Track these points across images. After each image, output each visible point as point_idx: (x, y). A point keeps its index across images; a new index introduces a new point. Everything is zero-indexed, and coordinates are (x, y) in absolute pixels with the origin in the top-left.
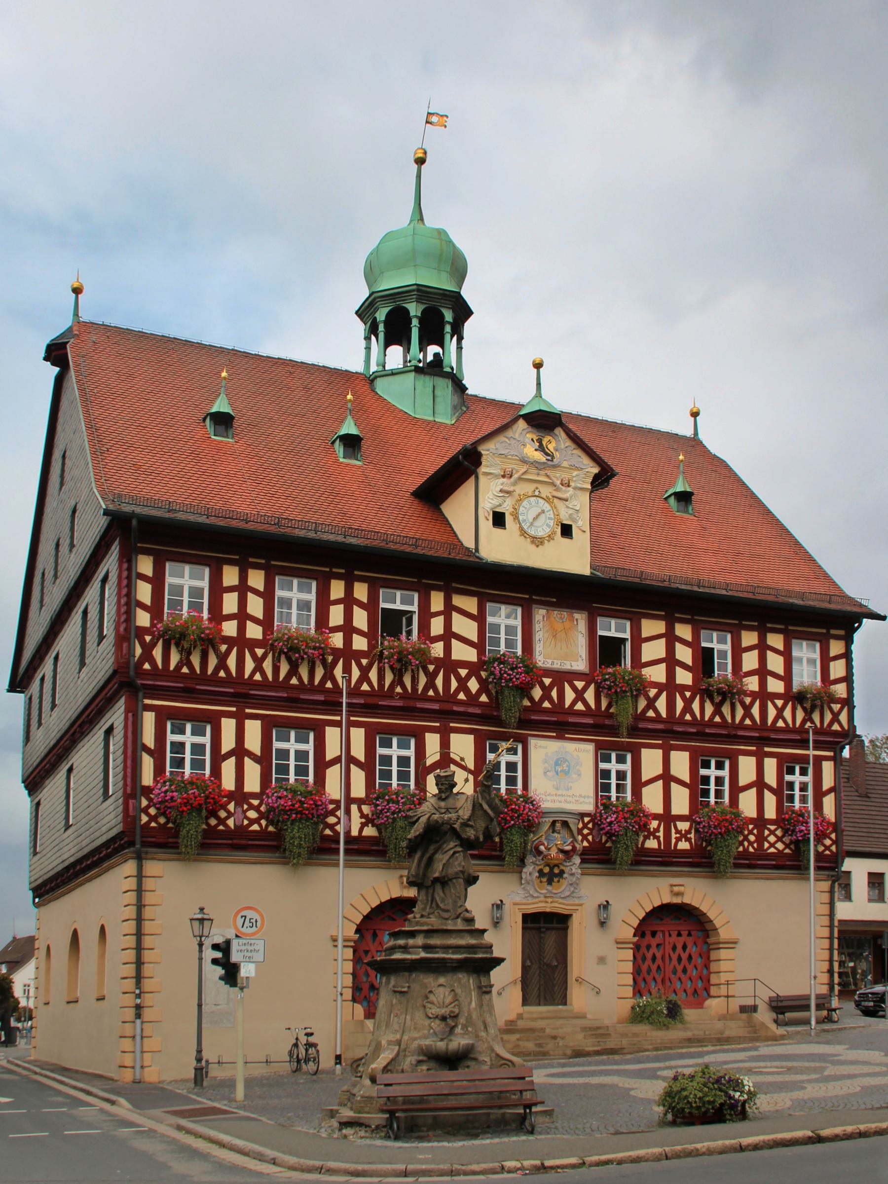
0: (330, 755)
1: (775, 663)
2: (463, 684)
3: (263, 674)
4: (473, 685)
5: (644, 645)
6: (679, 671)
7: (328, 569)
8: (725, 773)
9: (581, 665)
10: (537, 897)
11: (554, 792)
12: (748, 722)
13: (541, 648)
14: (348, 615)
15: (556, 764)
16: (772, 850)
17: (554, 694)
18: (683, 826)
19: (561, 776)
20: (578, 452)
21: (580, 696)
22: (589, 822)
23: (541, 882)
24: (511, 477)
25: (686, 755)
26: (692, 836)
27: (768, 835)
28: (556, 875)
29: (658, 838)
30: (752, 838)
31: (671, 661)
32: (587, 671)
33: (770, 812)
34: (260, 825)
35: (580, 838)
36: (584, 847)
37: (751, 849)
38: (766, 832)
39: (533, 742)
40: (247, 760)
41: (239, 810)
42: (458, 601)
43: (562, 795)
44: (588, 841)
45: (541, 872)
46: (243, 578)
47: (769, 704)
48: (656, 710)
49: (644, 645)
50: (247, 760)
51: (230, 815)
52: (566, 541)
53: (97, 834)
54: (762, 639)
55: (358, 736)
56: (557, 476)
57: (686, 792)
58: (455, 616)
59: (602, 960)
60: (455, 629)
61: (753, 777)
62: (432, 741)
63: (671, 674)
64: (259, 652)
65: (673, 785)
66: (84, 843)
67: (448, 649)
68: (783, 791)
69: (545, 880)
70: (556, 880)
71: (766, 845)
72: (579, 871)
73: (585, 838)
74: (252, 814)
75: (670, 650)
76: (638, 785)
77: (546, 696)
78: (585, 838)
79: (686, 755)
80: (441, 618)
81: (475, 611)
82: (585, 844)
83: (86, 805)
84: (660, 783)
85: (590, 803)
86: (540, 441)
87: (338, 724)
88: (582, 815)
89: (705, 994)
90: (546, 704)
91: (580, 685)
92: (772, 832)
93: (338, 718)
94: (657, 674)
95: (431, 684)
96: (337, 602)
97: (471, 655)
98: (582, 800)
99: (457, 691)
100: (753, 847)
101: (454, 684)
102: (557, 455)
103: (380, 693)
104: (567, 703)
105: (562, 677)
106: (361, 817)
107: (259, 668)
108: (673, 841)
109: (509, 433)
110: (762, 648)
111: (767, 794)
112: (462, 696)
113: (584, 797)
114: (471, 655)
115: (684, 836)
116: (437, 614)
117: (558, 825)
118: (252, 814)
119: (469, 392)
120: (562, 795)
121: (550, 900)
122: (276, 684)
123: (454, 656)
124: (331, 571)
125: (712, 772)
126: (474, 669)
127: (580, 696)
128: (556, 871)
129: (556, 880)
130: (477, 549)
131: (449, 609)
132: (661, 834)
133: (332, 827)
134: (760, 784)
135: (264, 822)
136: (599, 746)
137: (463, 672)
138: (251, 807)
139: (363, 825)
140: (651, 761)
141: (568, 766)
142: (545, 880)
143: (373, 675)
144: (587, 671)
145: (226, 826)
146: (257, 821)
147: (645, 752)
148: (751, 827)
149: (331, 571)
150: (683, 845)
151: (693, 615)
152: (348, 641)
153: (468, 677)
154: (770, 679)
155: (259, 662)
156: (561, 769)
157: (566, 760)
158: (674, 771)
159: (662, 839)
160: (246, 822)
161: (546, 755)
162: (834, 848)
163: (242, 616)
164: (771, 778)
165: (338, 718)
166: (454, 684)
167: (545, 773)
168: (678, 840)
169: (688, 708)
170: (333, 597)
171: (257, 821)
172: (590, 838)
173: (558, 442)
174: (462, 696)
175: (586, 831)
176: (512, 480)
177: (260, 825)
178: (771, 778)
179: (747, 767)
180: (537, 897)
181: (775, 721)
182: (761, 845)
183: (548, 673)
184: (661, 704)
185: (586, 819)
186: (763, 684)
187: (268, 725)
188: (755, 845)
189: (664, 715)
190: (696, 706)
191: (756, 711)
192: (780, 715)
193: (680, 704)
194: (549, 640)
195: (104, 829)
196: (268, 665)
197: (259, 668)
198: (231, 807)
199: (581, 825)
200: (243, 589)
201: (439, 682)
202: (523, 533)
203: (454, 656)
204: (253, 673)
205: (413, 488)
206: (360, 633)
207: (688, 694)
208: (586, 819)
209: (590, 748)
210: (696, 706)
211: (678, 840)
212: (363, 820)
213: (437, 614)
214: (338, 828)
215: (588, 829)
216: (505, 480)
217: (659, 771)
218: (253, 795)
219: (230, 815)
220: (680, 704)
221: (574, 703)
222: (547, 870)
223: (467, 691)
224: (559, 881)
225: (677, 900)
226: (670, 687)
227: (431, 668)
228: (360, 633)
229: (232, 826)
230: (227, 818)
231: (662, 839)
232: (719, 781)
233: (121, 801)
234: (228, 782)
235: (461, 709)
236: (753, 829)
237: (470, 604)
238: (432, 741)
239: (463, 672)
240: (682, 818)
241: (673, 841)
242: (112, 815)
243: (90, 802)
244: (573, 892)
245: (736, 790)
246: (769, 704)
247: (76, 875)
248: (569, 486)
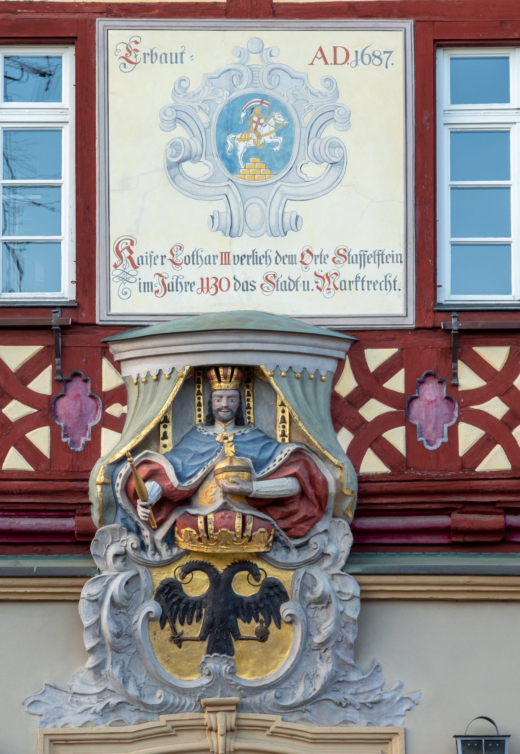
10: (163, 708)
11: (216, 243)
22: (388, 370)
35: (345, 438)
39: (115, 38)
43: (255, 259)
44: (386, 452)
45: (169, 593)
69: (194, 629)
72: (351, 587)
73: (368, 437)
78: (368, 437)
82: (372, 464)
85: (389, 284)
88: (359, 338)
98: (349, 271)
113: (363, 259)
120: (255, 259)
121: (220, 720)
128: (245, 588)
129: (247, 628)
142: (194, 629)
157: (275, 105)
161: (181, 86)
167: (174, 167)
172: (397, 437)
175: (373, 410)
180: (163, 708)
185: (376, 357)
208: (376, 357)
215: (387, 397)
222: (198, 586)
224: (262, 636)
244: (334, 682)
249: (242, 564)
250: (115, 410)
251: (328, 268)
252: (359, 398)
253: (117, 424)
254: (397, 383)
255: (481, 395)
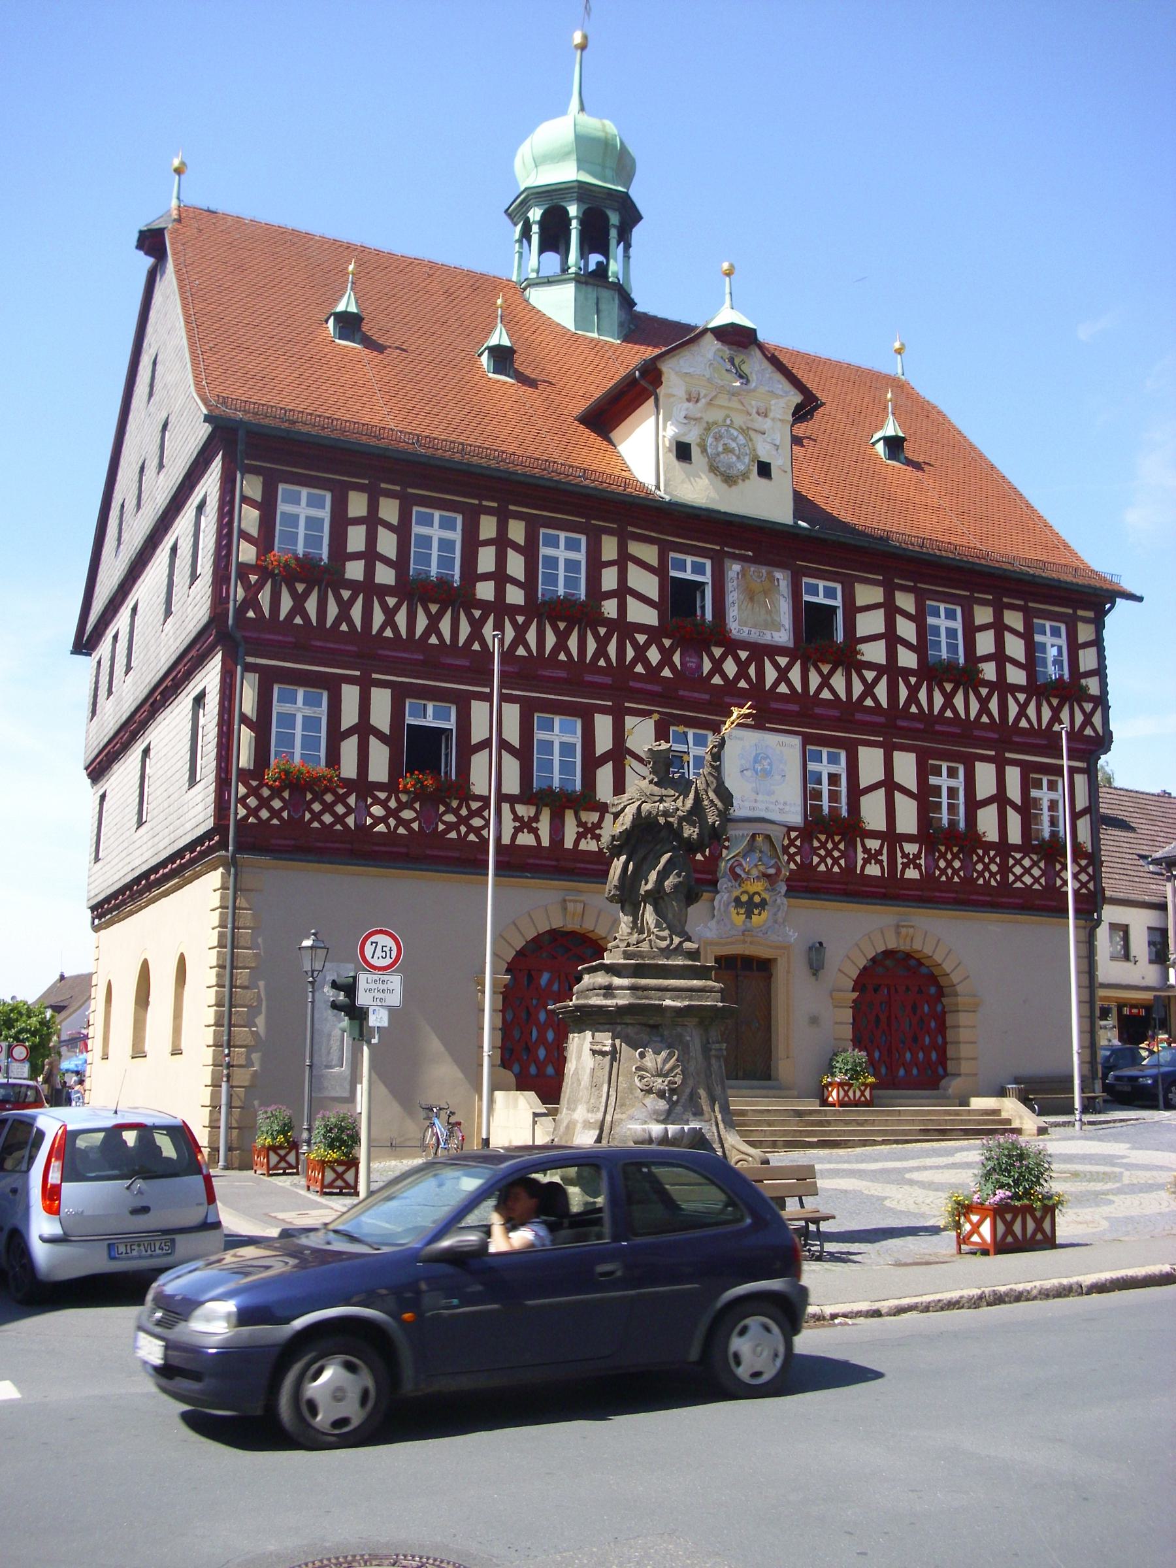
0: (477, 736)
1: (1015, 647)
2: (641, 651)
3: (395, 629)
4: (654, 655)
5: (858, 616)
6: (901, 650)
7: (477, 502)
8: (959, 783)
9: (783, 637)
12: (985, 719)
13: (736, 613)
14: (501, 560)
15: (756, 761)
16: (1018, 885)
17: (752, 671)
18: (911, 848)
19: (764, 775)
20: (778, 376)
21: (783, 675)
22: (796, 838)
23: (738, 914)
24: (697, 401)
25: (912, 757)
26: (922, 862)
27: (1014, 866)
28: (757, 906)
29: (881, 862)
30: (994, 868)
31: (891, 638)
32: (791, 645)
33: (1015, 836)
34: (388, 826)
35: (786, 858)
36: (791, 871)
37: (993, 883)
38: (1011, 862)
40: (373, 741)
41: (362, 804)
42: (635, 548)
44: (795, 863)
46: (373, 507)
47: (1010, 697)
48: (875, 699)
49: (858, 616)
50: (373, 741)
51: (349, 811)
52: (764, 481)
53: (180, 832)
54: (998, 616)
55: (512, 712)
56: (753, 404)
57: (913, 804)
58: (632, 568)
59: (814, 1020)
60: (632, 583)
61: (993, 791)
62: (603, 725)
63: (892, 654)
64: (391, 601)
65: (898, 796)
66: (162, 845)
67: (622, 609)
68: (1027, 809)
69: (742, 911)
70: (756, 912)
71: (1011, 878)
73: (791, 858)
74: (377, 810)
75: (890, 624)
76: (856, 793)
77: (742, 673)
78: (791, 858)
79: (912, 757)
80: (615, 569)
81: (654, 561)
82: (792, 866)
83: (166, 795)
84: (882, 791)
86: (732, 361)
87: (488, 698)
88: (791, 829)
89: (941, 1071)
90: (743, 684)
91: (783, 661)
92: (1018, 862)
93: (488, 690)
94: (875, 652)
95: (601, 651)
96: (487, 543)
97: (650, 617)
99: (634, 662)
100: (996, 880)
101: (630, 653)
102: (754, 378)
103: (539, 660)
104: (768, 684)
105: (761, 652)
106: (514, 820)
107: (390, 621)
108: (900, 867)
109: (694, 348)
110: (999, 628)
111: (1010, 812)
112: (639, 669)
114: (650, 617)
115: (912, 861)
116: (610, 564)
117: (759, 839)
118: (377, 810)
119: (638, 308)
122: (412, 642)
123: (631, 618)
124: (480, 505)
125: (943, 782)
126: (656, 635)
127: (783, 675)
130: (658, 487)
131: (623, 560)
132: (884, 858)
133: (477, 831)
134: (1000, 799)
135: (392, 822)
136: (807, 740)
137: (641, 638)
138: (377, 801)
139: (517, 831)
140: (871, 763)
141: (769, 764)
142: (742, 911)
143: (531, 636)
144: (791, 645)
145: (345, 825)
146: (383, 820)
147: (863, 751)
148: (992, 853)
149: (480, 505)
150: (912, 874)
151: (915, 582)
152: (500, 592)
153: (647, 645)
154: (1009, 667)
155: (390, 614)
156: (761, 768)
157: (768, 757)
158: (898, 778)
159: (885, 864)
160: (369, 821)
162: (1091, 886)
163: (371, 556)
164: (1014, 792)
165: (488, 690)
166: (630, 653)
168: (905, 866)
169: (913, 698)
170: (483, 536)
171: (383, 820)
173: (755, 364)
174: (639, 669)
175: (792, 850)
176: (699, 405)
177: (388, 826)
178: (1014, 792)
179: (985, 778)
181: (1017, 719)
182: (1005, 877)
183: (745, 645)
184: (881, 691)
185: (793, 834)
186: (1001, 672)
187: (399, 696)
188: (998, 877)
189: (885, 706)
190: (922, 695)
191: (993, 706)
192: (1022, 713)
193: (903, 693)
194: (745, 604)
195: (189, 826)
196: (401, 619)
197: (390, 621)
198: (352, 800)
199: (786, 842)
200: (372, 521)
201: (612, 649)
202: (714, 469)
203: (631, 618)
204: (382, 628)
205: (577, 412)
206: (515, 582)
207: (913, 680)
208: (793, 834)
209: (796, 741)
210: (922, 695)
211: (905, 866)
212: (517, 824)
213: (610, 564)
214: (484, 833)
215: (796, 847)
216: (690, 405)
217: (881, 776)
218: (380, 786)
219: (349, 811)
220: (903, 693)
221: (776, 684)
222: (744, 898)
223: (646, 663)
225: (904, 947)
226: (891, 670)
227: (602, 631)
228: (515, 582)
229: (352, 825)
230: (346, 815)
231: (885, 864)
232: (952, 792)
233: (213, 787)
234: (349, 768)
235: (639, 685)
236: (995, 856)
237: (649, 553)
238: (603, 725)
239: (641, 638)
240: (909, 838)
241: (900, 867)
242: (200, 807)
243: (171, 791)
245: (973, 805)
246: (1010, 697)
247: (149, 887)
248: (766, 416)
249: (757, 893)
250: (726, 844)
251: (781, 807)
252: (789, 846)
253: (727, 848)
254: (798, 843)
255: (819, 848)
